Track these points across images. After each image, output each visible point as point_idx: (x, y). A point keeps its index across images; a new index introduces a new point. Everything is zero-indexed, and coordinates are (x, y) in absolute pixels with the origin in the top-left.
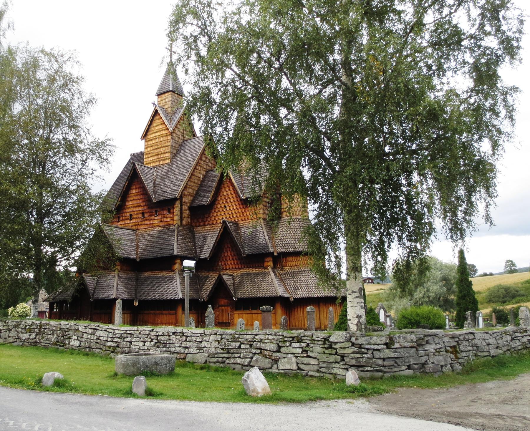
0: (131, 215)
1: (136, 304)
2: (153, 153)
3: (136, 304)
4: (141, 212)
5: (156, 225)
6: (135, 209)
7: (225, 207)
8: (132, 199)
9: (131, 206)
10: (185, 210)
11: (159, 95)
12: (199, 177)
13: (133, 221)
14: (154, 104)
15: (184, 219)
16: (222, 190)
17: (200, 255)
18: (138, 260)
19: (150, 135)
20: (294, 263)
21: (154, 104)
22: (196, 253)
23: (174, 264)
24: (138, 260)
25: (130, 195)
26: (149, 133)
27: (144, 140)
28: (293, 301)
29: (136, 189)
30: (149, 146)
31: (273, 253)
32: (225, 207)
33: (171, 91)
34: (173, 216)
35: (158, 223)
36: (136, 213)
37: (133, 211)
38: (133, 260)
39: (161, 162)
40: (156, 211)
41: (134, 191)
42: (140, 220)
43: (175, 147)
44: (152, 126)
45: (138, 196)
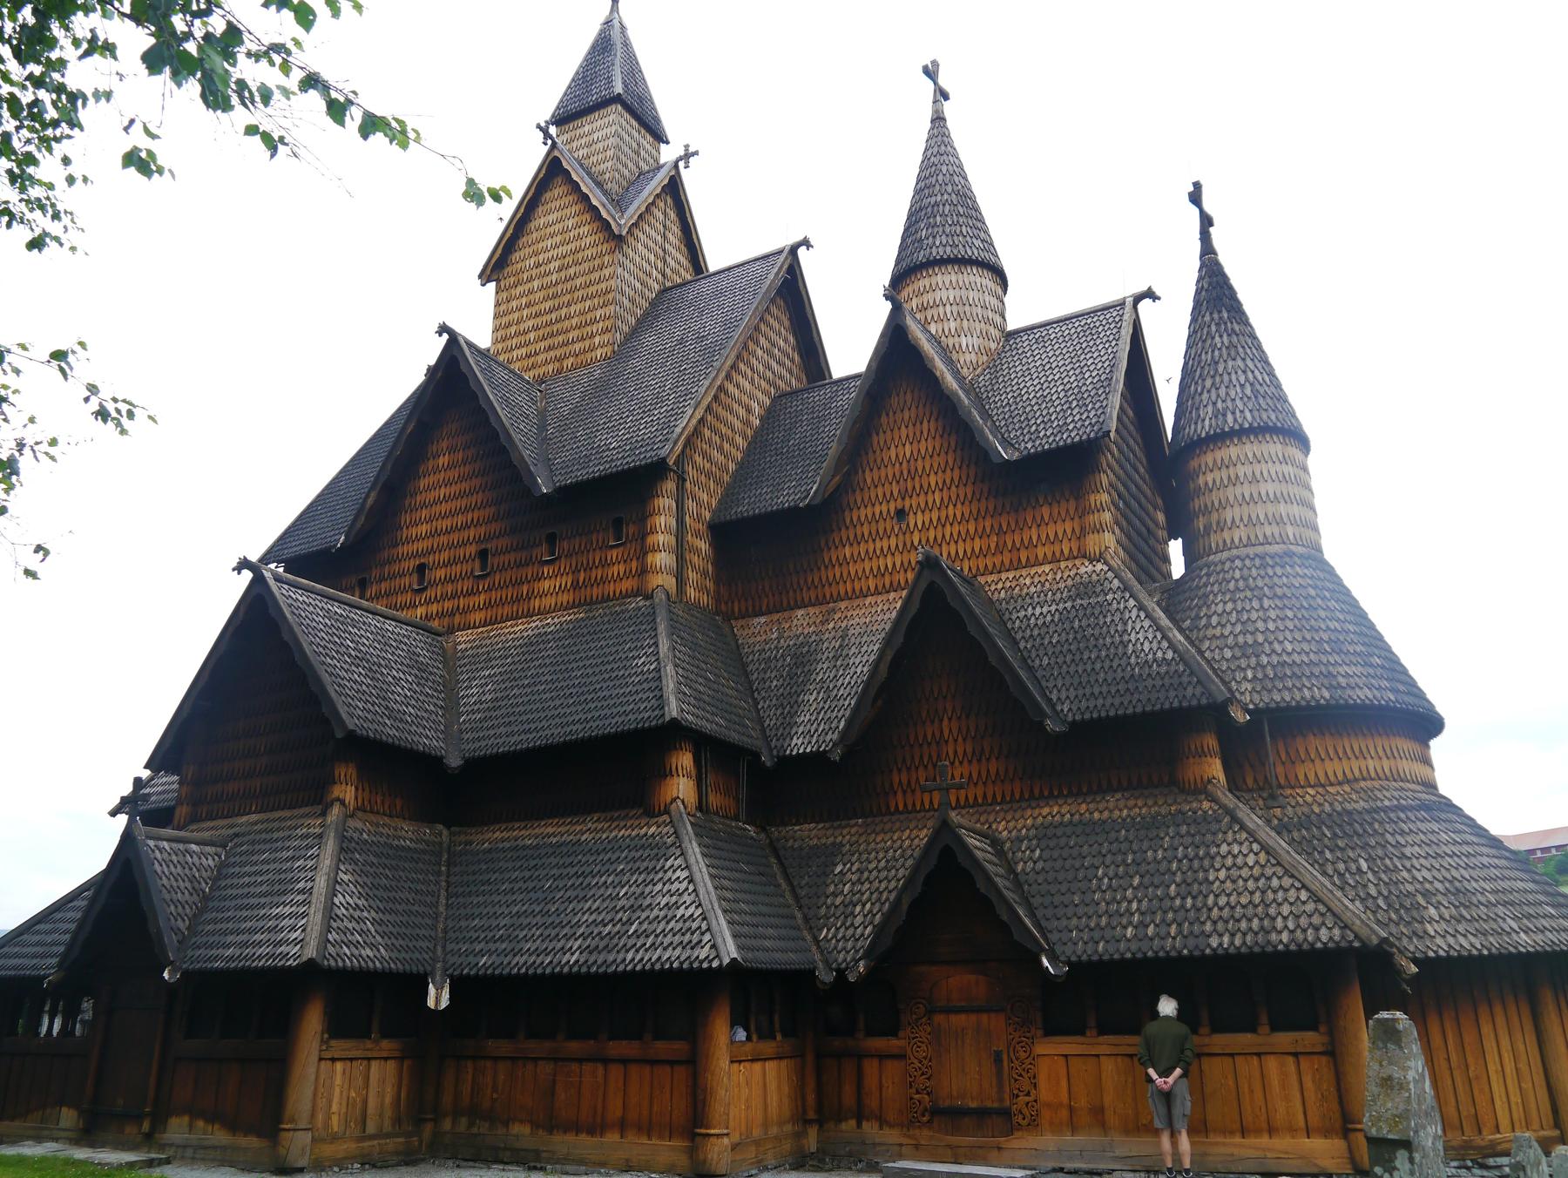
0: (421, 569)
1: (438, 997)
2: (536, 328)
3: (438, 997)
4: (472, 549)
5: (549, 601)
6: (444, 539)
7: (901, 514)
8: (432, 495)
9: (424, 528)
10: (697, 534)
12: (749, 410)
13: (430, 593)
15: (692, 576)
16: (878, 440)
18: (454, 761)
19: (523, 258)
20: (1334, 768)
23: (664, 773)
24: (454, 761)
25: (423, 483)
26: (516, 256)
27: (492, 286)
29: (452, 450)
30: (514, 304)
32: (901, 514)
33: (617, 99)
34: (644, 552)
35: (562, 590)
36: (445, 556)
37: (431, 551)
38: (428, 763)
39: (568, 362)
40: (552, 539)
41: (443, 460)
42: (467, 585)
43: (632, 301)
44: (532, 225)
45: (461, 479)
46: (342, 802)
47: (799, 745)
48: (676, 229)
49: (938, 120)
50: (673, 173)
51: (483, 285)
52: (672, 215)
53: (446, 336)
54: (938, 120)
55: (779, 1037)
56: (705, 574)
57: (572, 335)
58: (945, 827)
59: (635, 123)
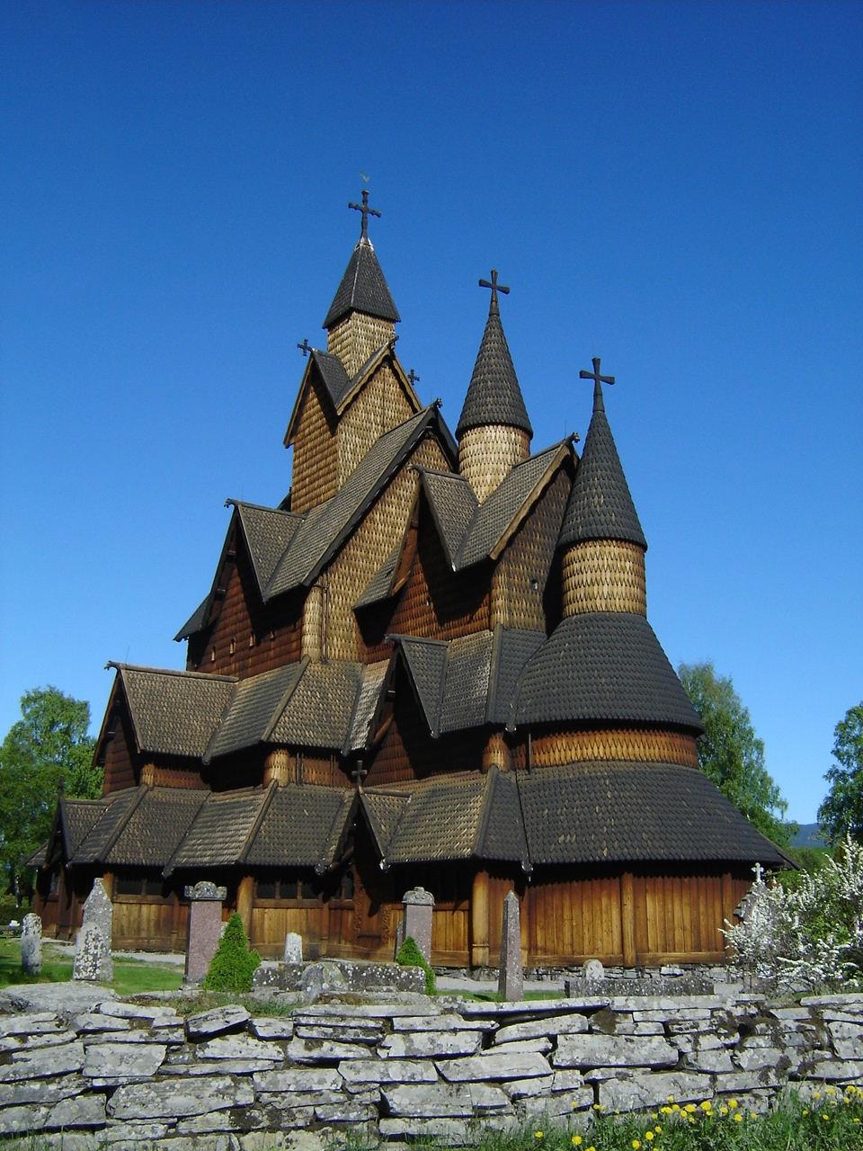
10: (343, 616)
11: (331, 325)
12: (394, 526)
14: (305, 347)
17: (354, 739)
21: (305, 347)
22: (348, 735)
24: (207, 759)
28: (532, 874)
31: (504, 725)
34: (302, 635)
38: (198, 760)
46: (147, 784)
47: (359, 744)
48: (395, 389)
49: (494, 314)
50: (387, 352)
51: (287, 447)
52: (392, 379)
53: (232, 506)
54: (494, 314)
55: (299, 897)
56: (348, 639)
57: (321, 481)
58: (358, 794)
59: (369, 319)
